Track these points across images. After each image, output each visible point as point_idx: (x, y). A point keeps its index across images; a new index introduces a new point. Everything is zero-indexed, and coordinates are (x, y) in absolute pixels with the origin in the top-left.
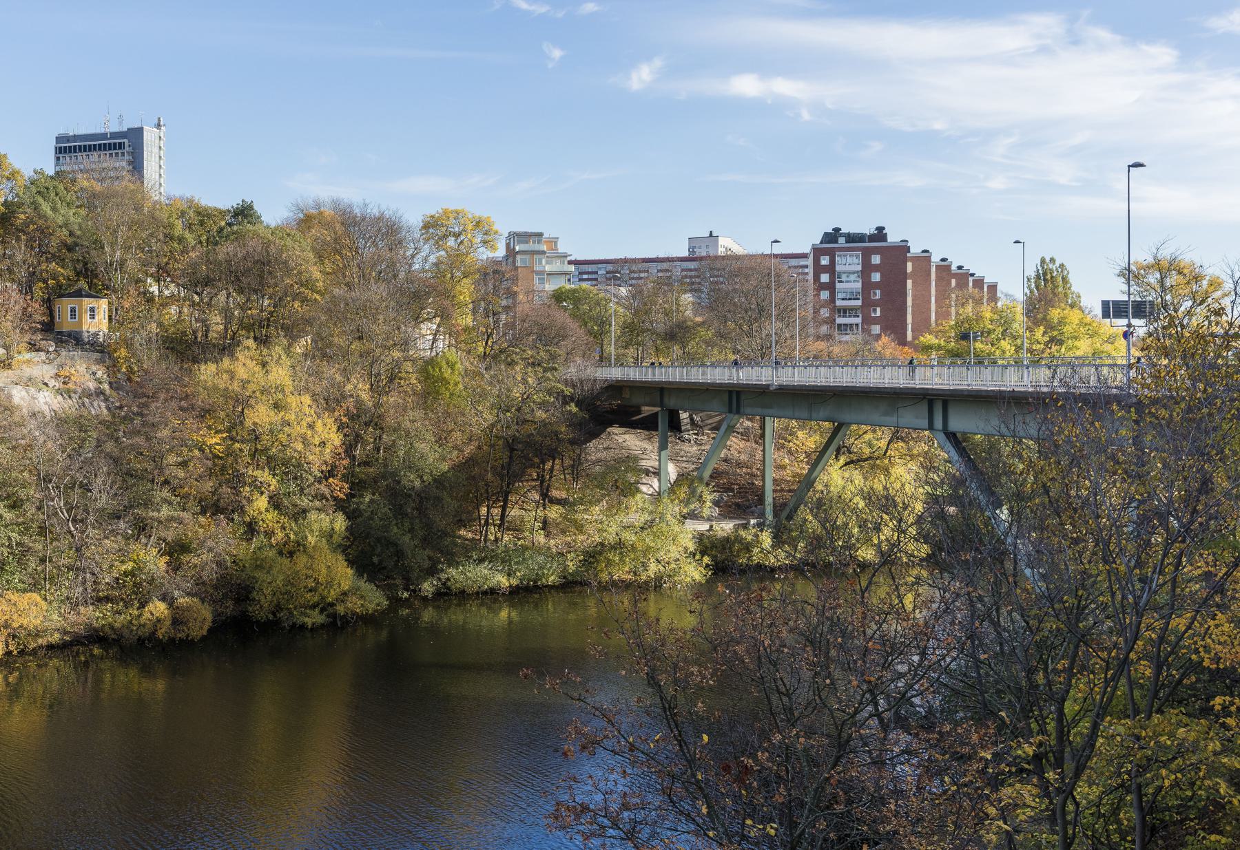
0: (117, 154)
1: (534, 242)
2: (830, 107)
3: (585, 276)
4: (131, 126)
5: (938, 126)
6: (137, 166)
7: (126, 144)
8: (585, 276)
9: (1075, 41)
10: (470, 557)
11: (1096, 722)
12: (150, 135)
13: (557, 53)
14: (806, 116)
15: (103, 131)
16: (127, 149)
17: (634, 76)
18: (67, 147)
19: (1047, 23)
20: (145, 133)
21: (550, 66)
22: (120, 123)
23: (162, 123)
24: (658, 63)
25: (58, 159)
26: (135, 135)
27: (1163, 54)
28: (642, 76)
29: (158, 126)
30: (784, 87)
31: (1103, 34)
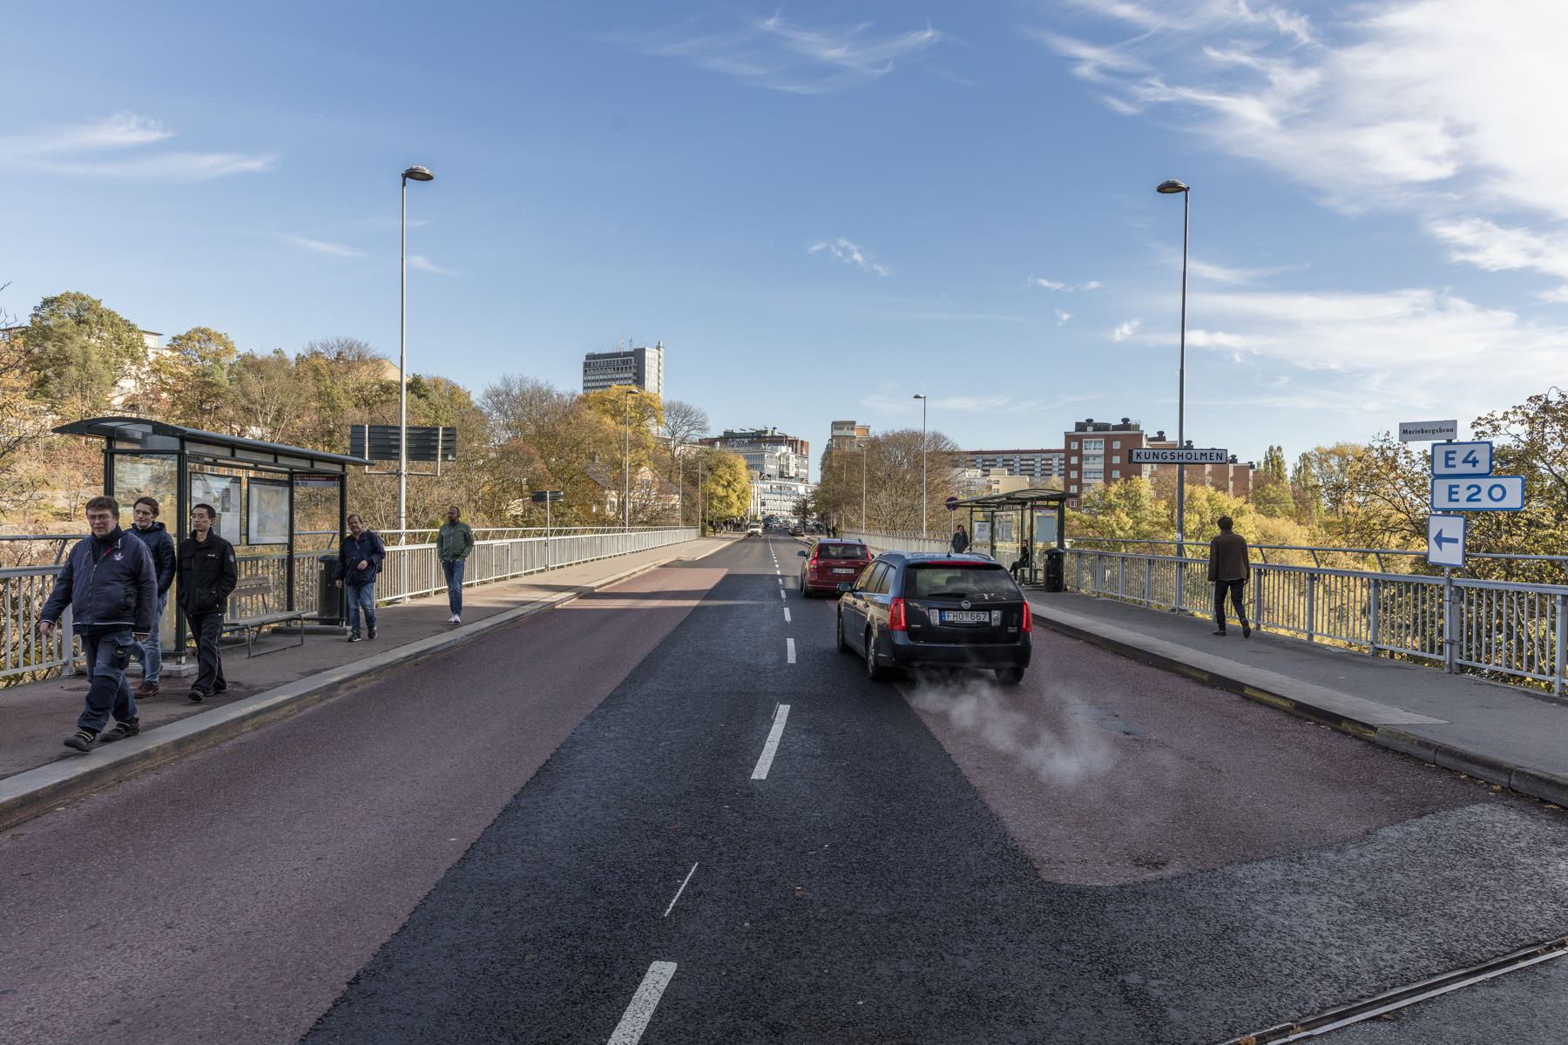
0: (622, 369)
1: (848, 429)
2: (1255, 353)
3: (987, 463)
4: (636, 347)
5: (1333, 366)
6: (639, 380)
7: (633, 361)
8: (987, 463)
9: (1441, 308)
10: (913, 667)
11: (1460, 757)
12: (651, 355)
13: (1066, 317)
14: (1238, 359)
15: (618, 351)
16: (633, 364)
17: (1117, 332)
18: (594, 363)
19: (1420, 295)
20: (646, 353)
21: (1060, 324)
22: (631, 345)
23: (661, 345)
24: (1136, 323)
25: (586, 371)
26: (639, 354)
27: (1506, 317)
28: (1123, 332)
29: (658, 348)
30: (1223, 339)
31: (1461, 303)
